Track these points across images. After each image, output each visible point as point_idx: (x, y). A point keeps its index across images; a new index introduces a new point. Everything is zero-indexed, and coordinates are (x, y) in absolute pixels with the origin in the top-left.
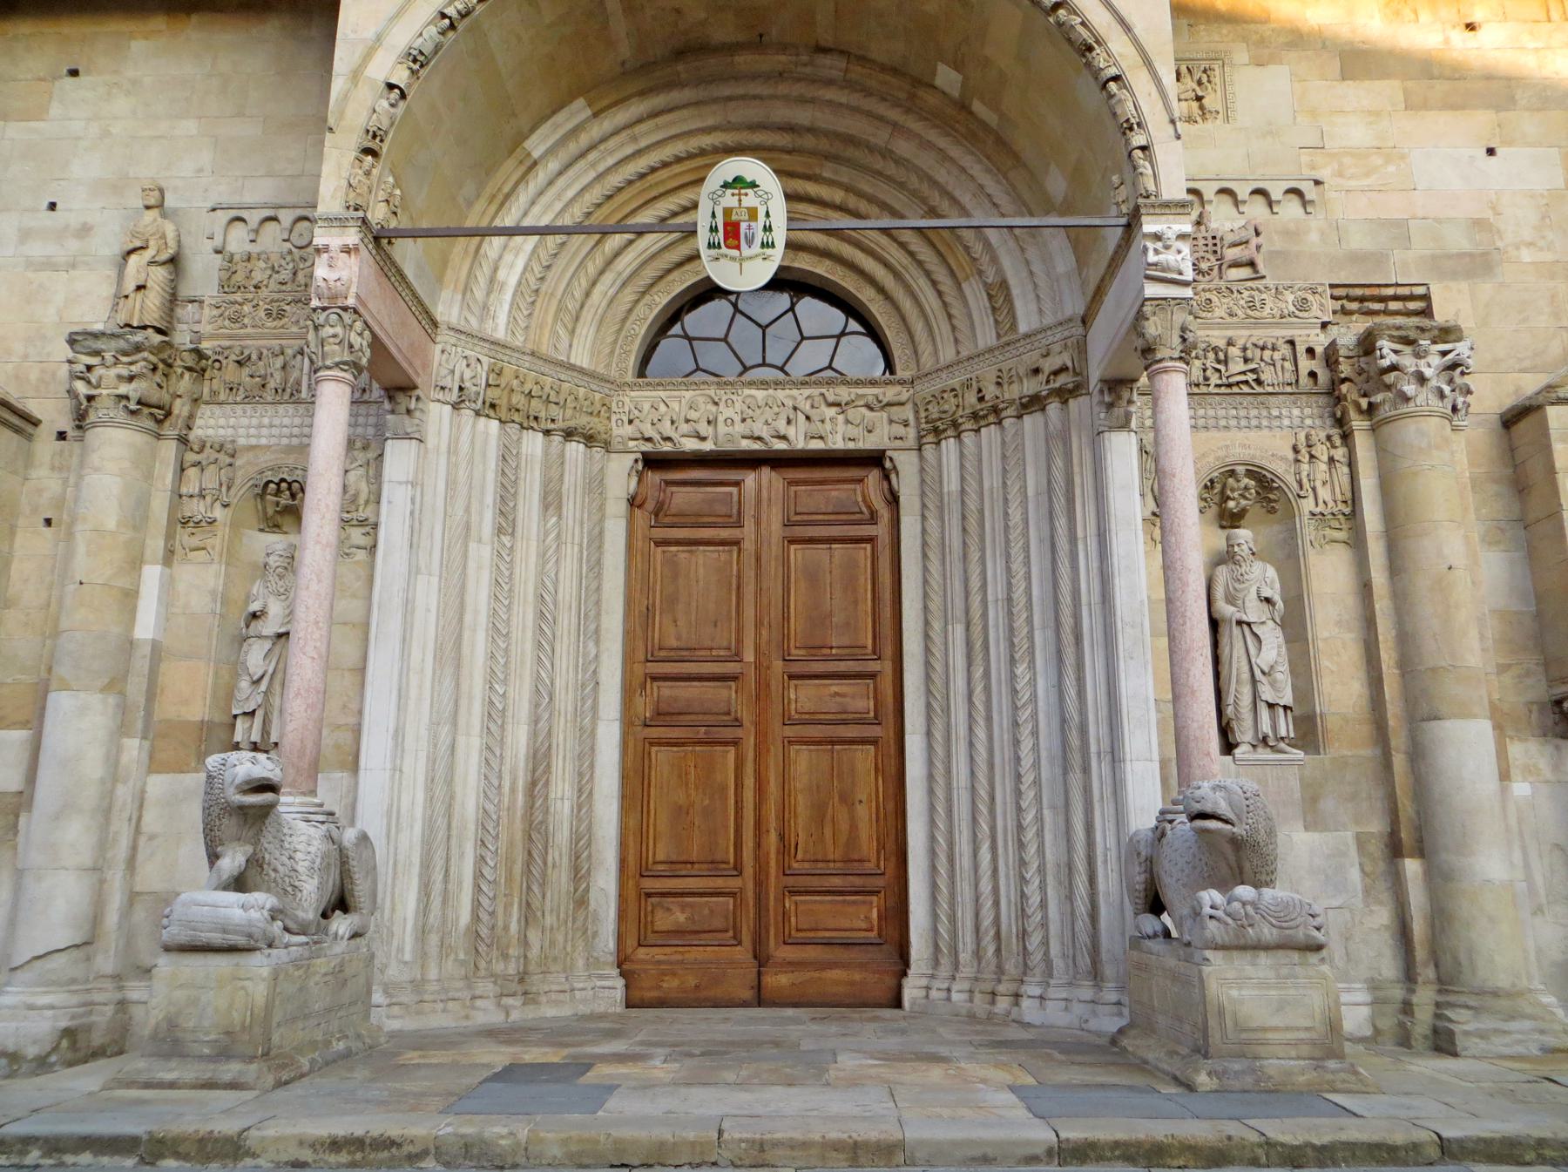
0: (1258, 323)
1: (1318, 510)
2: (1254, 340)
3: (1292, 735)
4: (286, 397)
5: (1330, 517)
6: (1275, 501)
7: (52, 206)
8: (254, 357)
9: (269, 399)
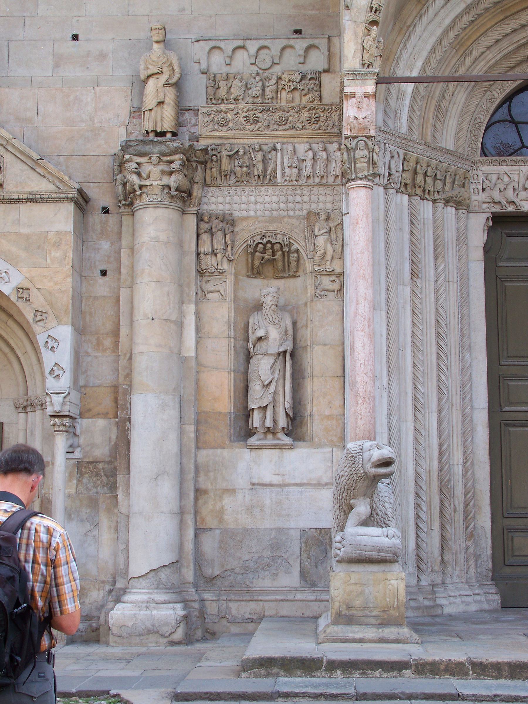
7: (75, 37)
8: (241, 152)
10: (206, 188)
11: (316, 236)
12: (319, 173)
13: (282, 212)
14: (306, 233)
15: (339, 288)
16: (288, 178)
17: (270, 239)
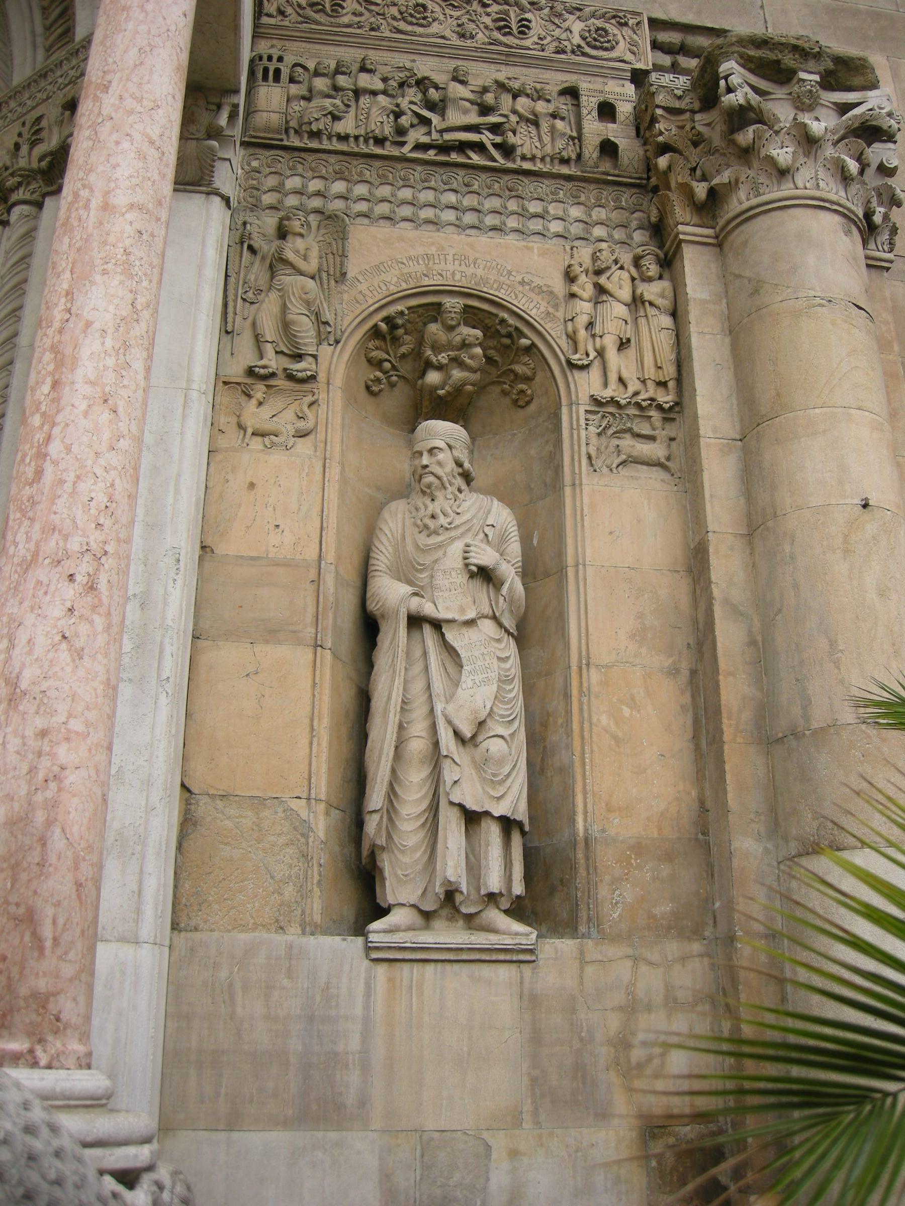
0: (510, 57)
1: (608, 393)
2: (501, 77)
3: (518, 888)
5: (632, 411)
6: (528, 379)
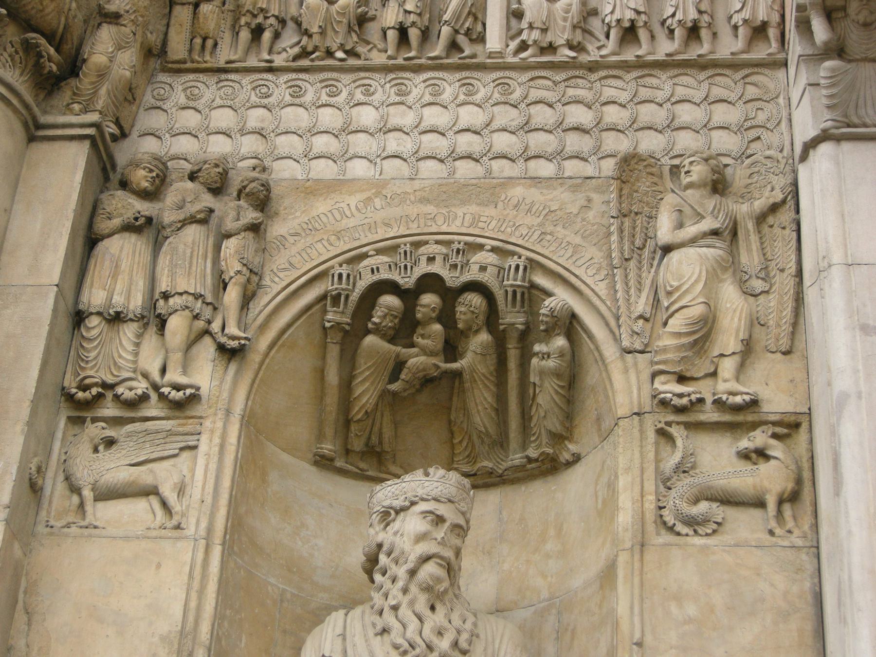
4: (438, 49)
9: (379, 58)
10: (163, 77)
11: (667, 249)
12: (679, 16)
13: (496, 165)
14: (614, 238)
15: (790, 486)
16: (535, 35)
17: (436, 268)
